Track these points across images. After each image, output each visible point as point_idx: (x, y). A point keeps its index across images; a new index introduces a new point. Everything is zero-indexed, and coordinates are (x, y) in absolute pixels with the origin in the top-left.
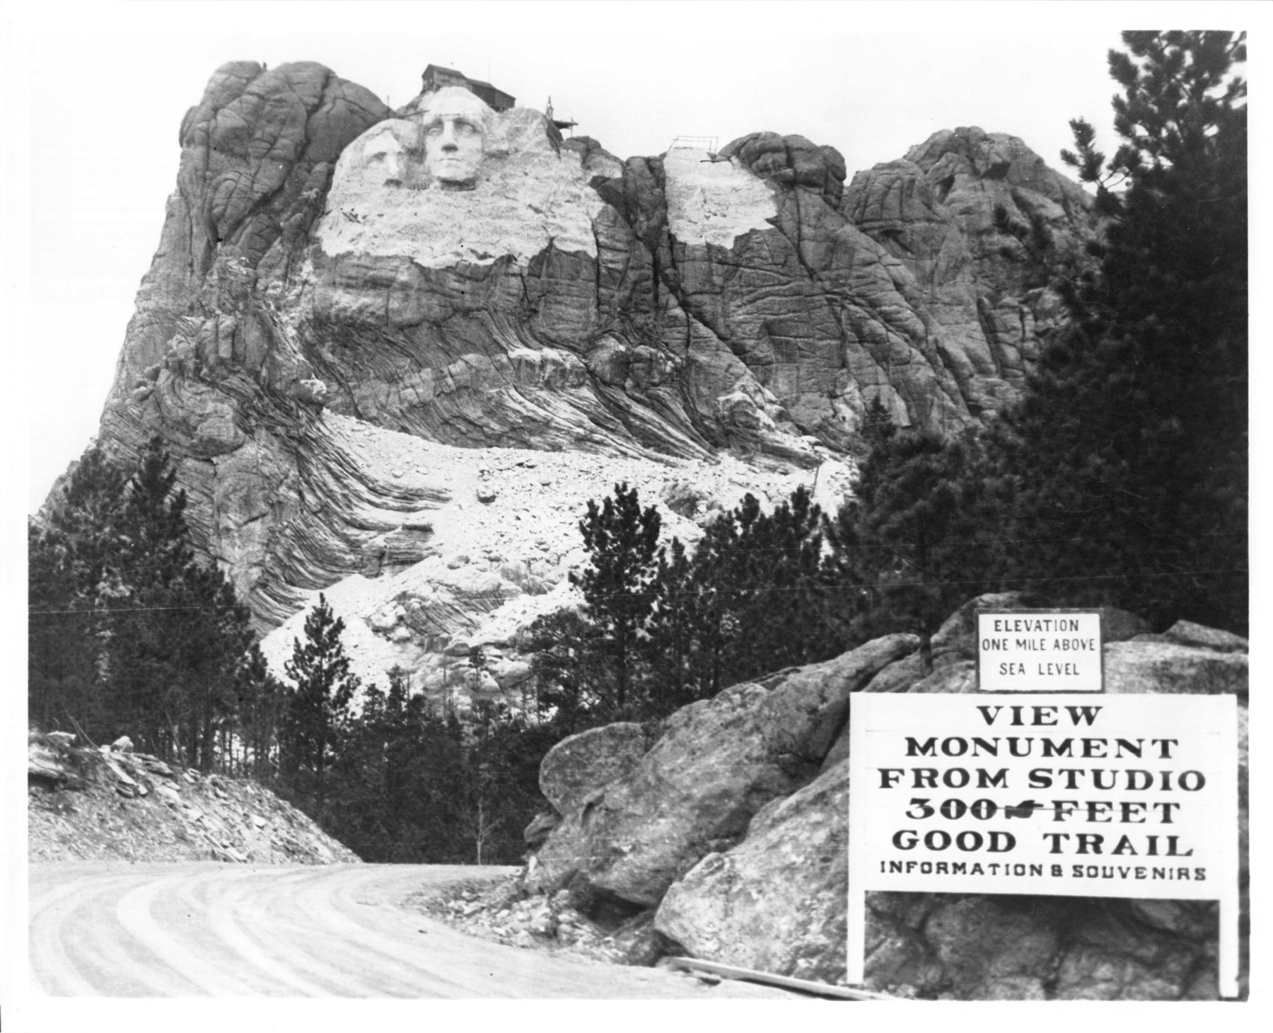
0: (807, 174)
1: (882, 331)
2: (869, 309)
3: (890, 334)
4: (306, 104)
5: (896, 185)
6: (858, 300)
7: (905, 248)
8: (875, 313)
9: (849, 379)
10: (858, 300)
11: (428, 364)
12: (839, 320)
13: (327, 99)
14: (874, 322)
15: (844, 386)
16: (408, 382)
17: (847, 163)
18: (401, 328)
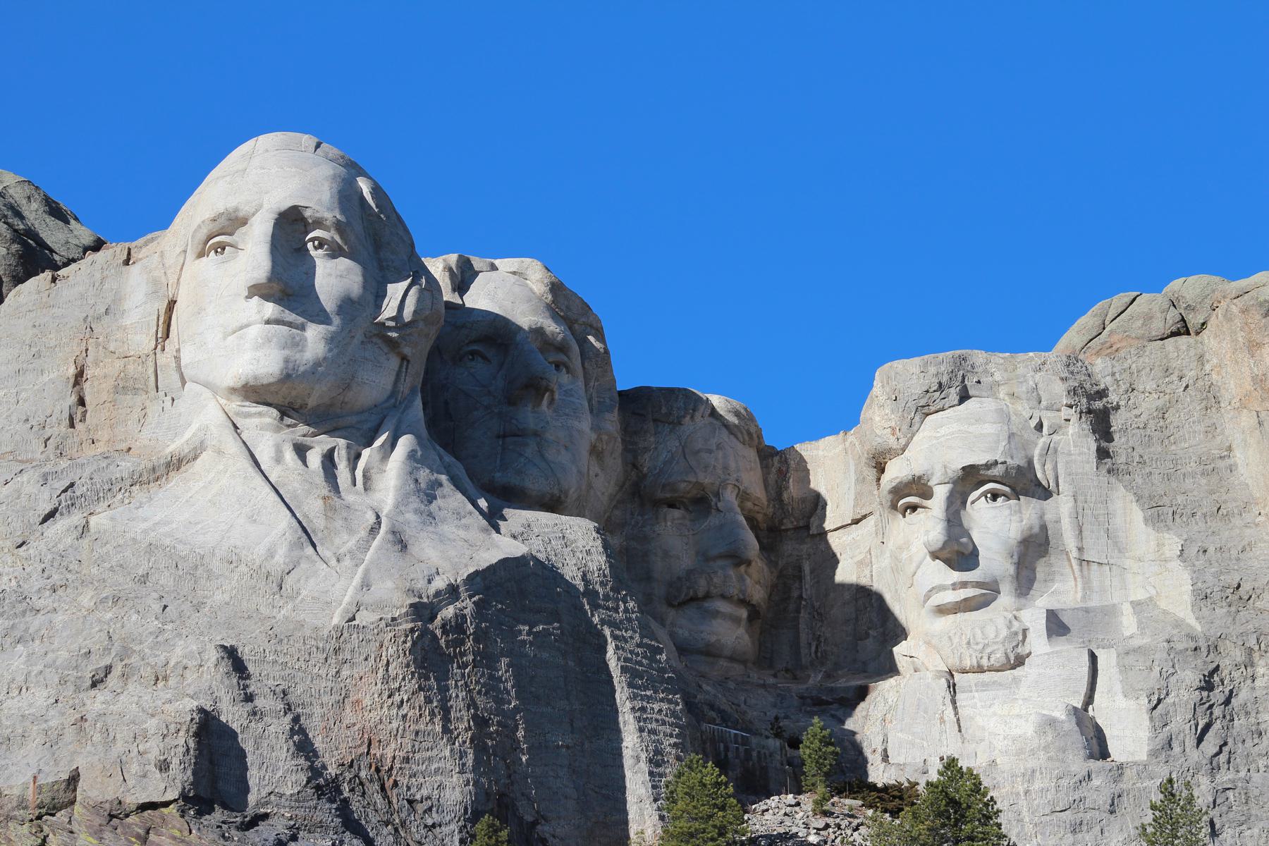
18: (115, 815)
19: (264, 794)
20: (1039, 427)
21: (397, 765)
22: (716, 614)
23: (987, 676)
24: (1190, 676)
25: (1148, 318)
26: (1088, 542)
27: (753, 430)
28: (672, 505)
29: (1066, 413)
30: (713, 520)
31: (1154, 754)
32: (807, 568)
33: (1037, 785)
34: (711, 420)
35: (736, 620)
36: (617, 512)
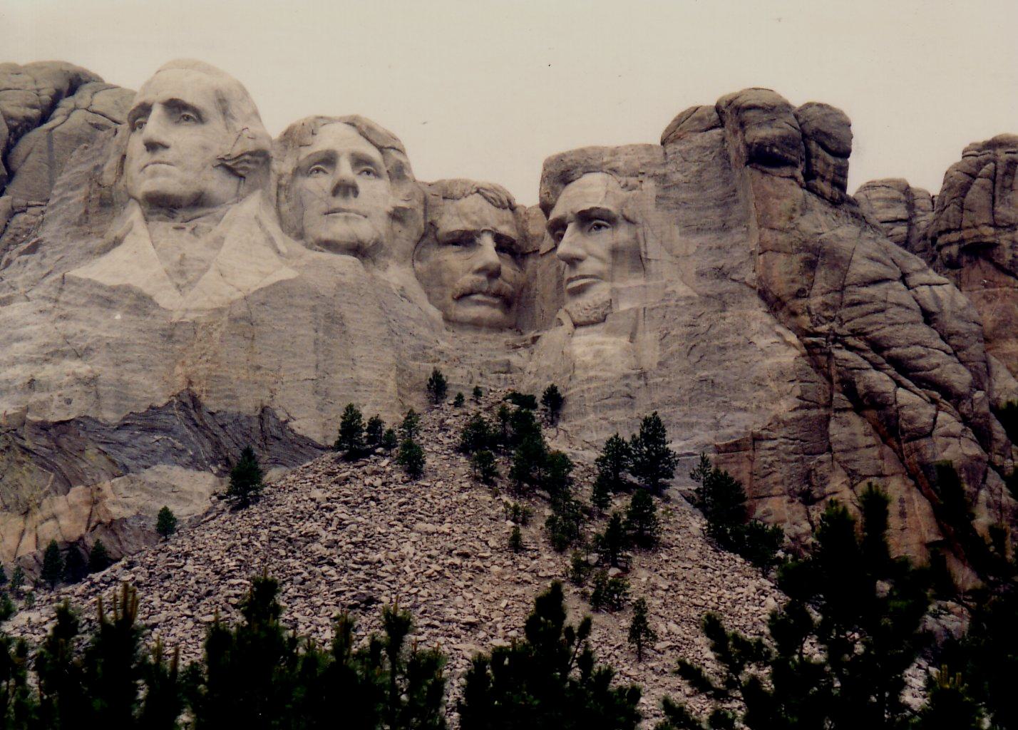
0: (760, 144)
1: (889, 386)
2: (870, 355)
3: (901, 391)
4: (8, 118)
5: (984, 170)
6: (851, 341)
7: (1000, 268)
8: (880, 359)
9: (832, 470)
10: (851, 341)
11: (80, 480)
12: (829, 378)
13: (58, 112)
14: (874, 376)
15: (824, 481)
16: (46, 511)
17: (854, 129)
18: (44, 427)
19: (128, 412)
20: (626, 185)
21: (204, 395)
22: (479, 303)
23: (590, 328)
24: (687, 318)
25: (701, 119)
26: (649, 249)
27: (504, 199)
28: (455, 243)
29: (641, 177)
30: (480, 251)
31: (660, 364)
32: (539, 272)
33: (593, 385)
34: (477, 195)
35: (494, 306)
36: (425, 250)
